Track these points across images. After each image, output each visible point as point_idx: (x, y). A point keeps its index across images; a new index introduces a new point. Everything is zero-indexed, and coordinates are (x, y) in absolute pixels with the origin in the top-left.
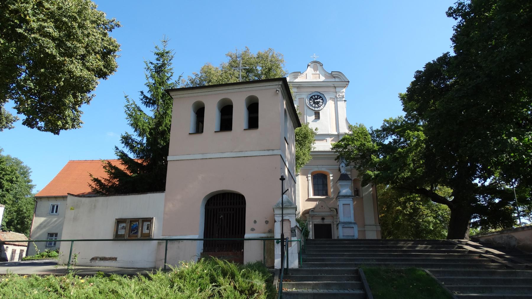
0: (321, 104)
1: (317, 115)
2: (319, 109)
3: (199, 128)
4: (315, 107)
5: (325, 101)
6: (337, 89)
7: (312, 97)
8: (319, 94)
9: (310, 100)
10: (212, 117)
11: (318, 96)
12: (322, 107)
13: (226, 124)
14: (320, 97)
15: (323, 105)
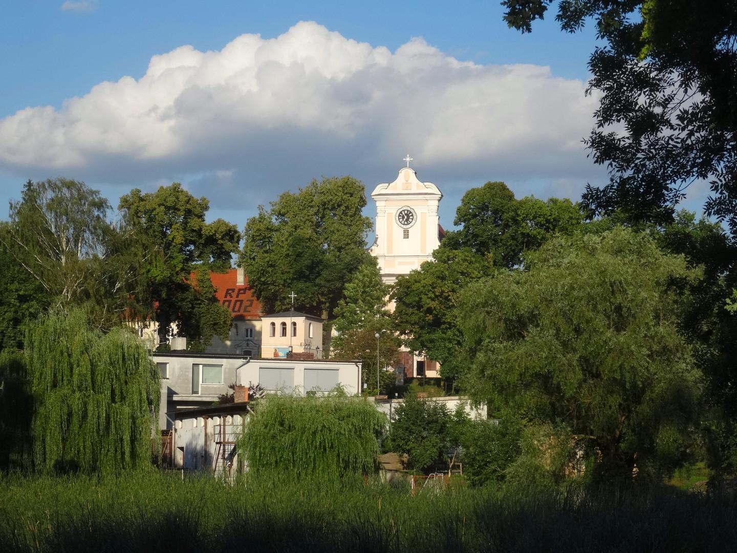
0: (410, 220)
1: (406, 235)
2: (408, 226)
3: (274, 335)
4: (404, 224)
5: (415, 217)
6: (430, 203)
7: (401, 213)
8: (409, 209)
9: (399, 216)
10: (278, 328)
11: (408, 211)
12: (411, 224)
13: (284, 334)
14: (411, 212)
15: (414, 222)
